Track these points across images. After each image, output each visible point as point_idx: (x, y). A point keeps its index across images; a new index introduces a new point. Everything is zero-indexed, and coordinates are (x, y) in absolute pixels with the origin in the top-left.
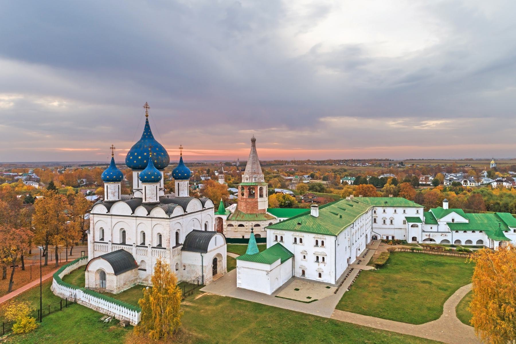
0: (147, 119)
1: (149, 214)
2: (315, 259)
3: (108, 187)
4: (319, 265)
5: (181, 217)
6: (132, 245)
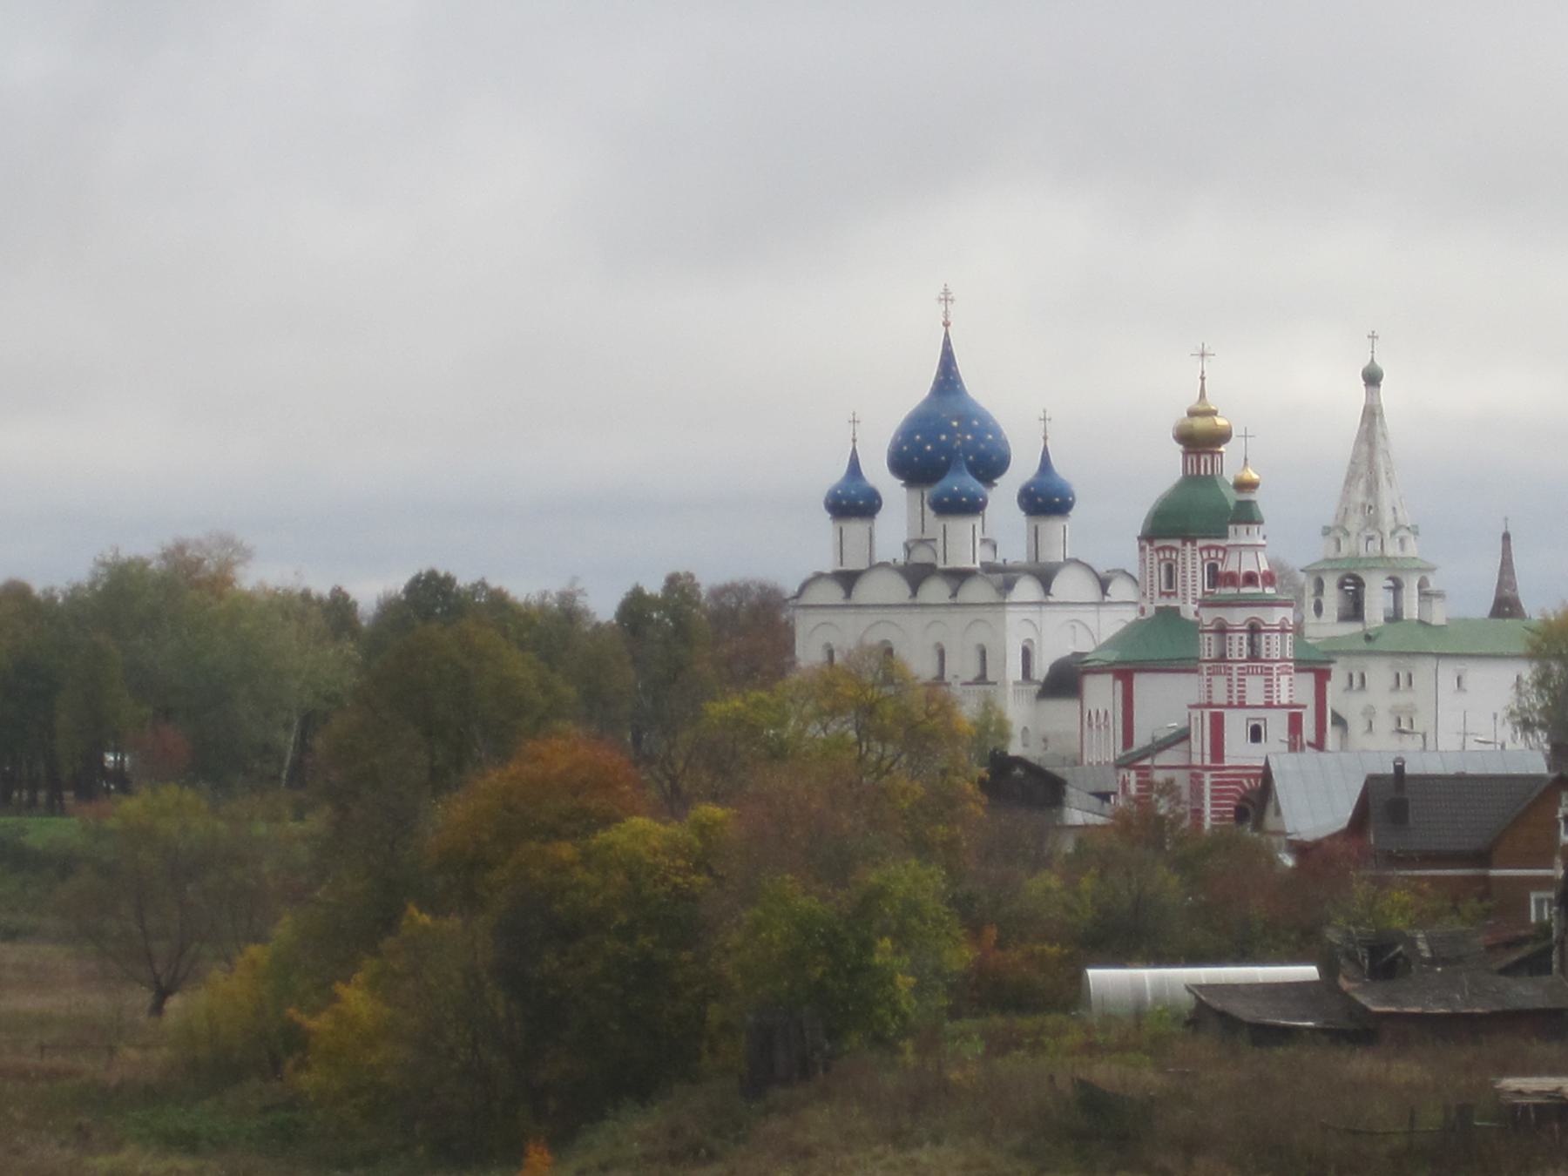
0: (947, 335)
1: (954, 595)
3: (844, 529)
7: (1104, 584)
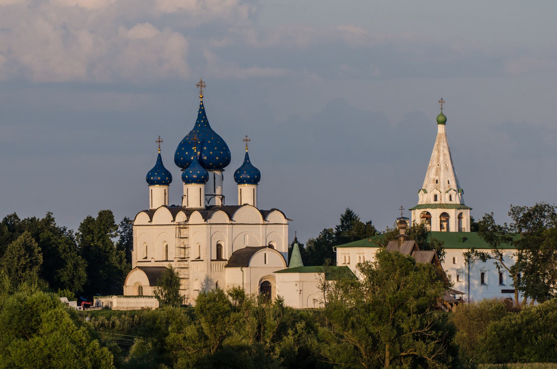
6: (173, 261)
7: (265, 214)
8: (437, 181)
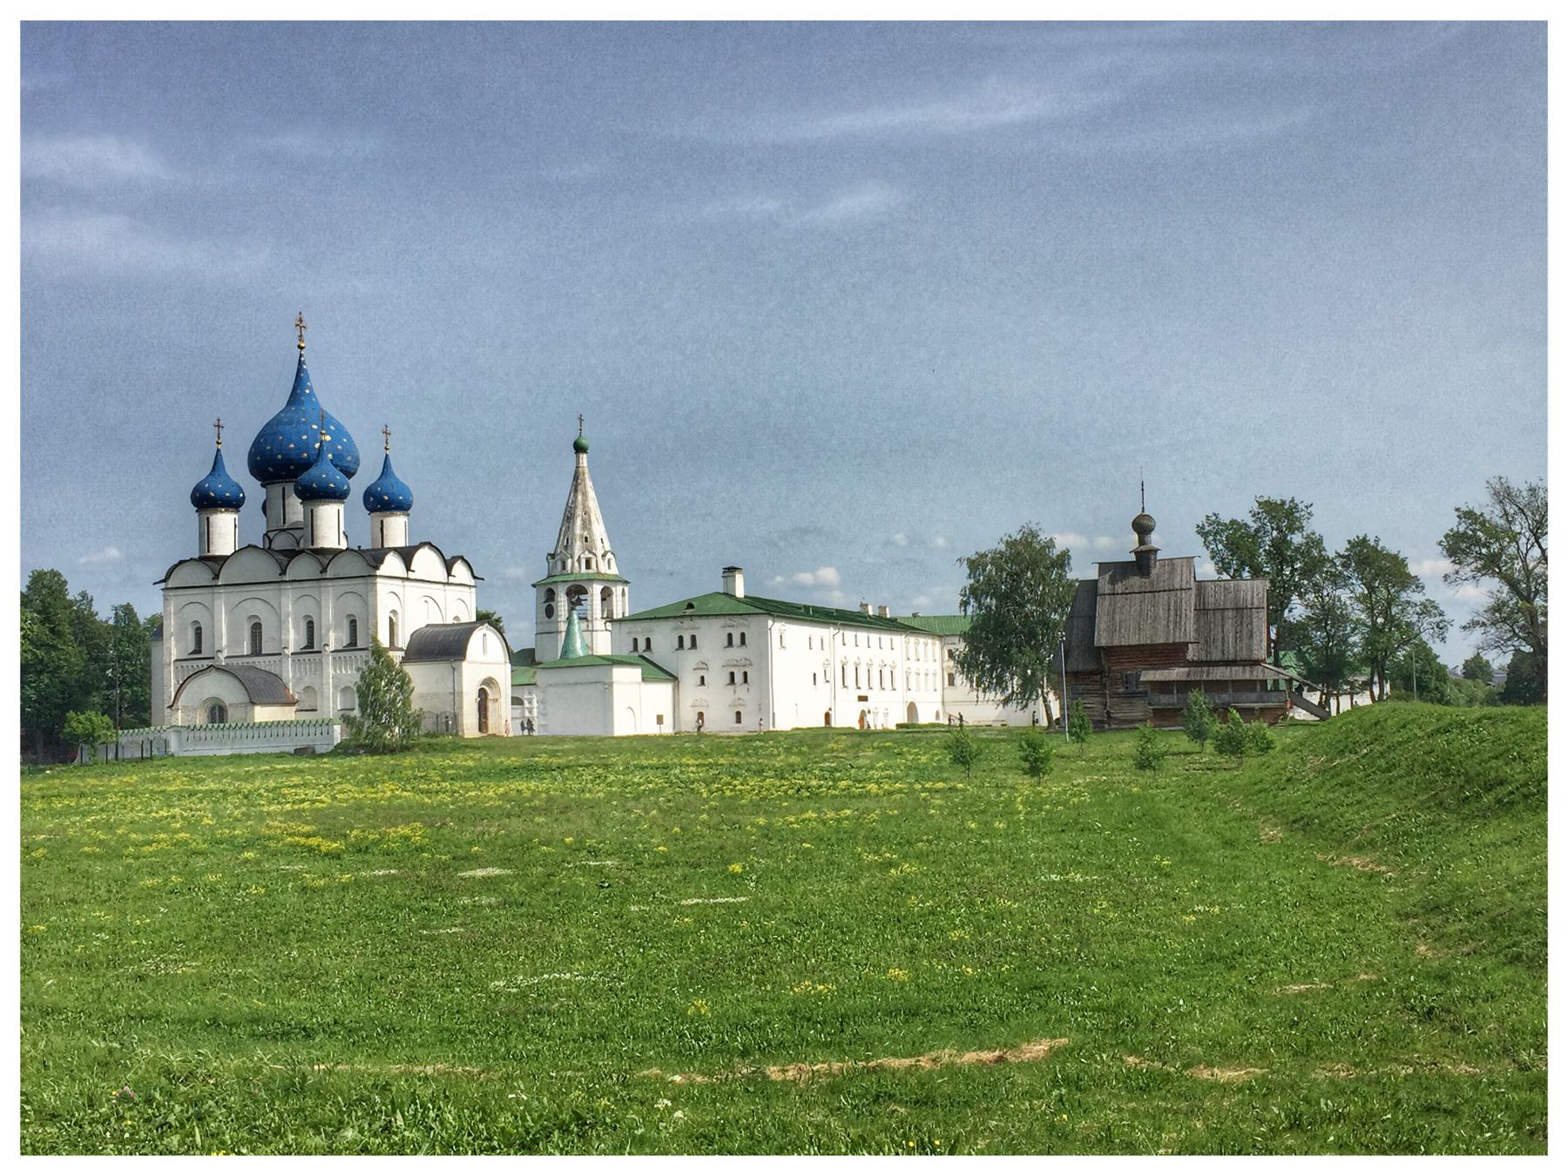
2: (728, 680)
4: (735, 691)
5: (399, 582)
6: (280, 654)
7: (449, 566)
8: (586, 538)
